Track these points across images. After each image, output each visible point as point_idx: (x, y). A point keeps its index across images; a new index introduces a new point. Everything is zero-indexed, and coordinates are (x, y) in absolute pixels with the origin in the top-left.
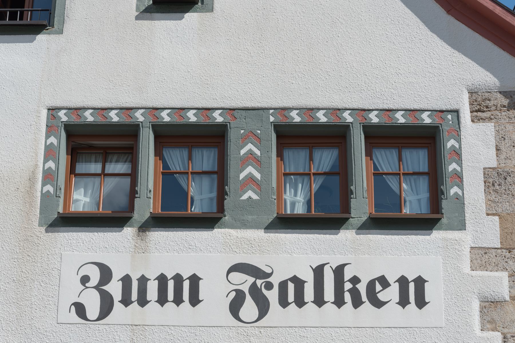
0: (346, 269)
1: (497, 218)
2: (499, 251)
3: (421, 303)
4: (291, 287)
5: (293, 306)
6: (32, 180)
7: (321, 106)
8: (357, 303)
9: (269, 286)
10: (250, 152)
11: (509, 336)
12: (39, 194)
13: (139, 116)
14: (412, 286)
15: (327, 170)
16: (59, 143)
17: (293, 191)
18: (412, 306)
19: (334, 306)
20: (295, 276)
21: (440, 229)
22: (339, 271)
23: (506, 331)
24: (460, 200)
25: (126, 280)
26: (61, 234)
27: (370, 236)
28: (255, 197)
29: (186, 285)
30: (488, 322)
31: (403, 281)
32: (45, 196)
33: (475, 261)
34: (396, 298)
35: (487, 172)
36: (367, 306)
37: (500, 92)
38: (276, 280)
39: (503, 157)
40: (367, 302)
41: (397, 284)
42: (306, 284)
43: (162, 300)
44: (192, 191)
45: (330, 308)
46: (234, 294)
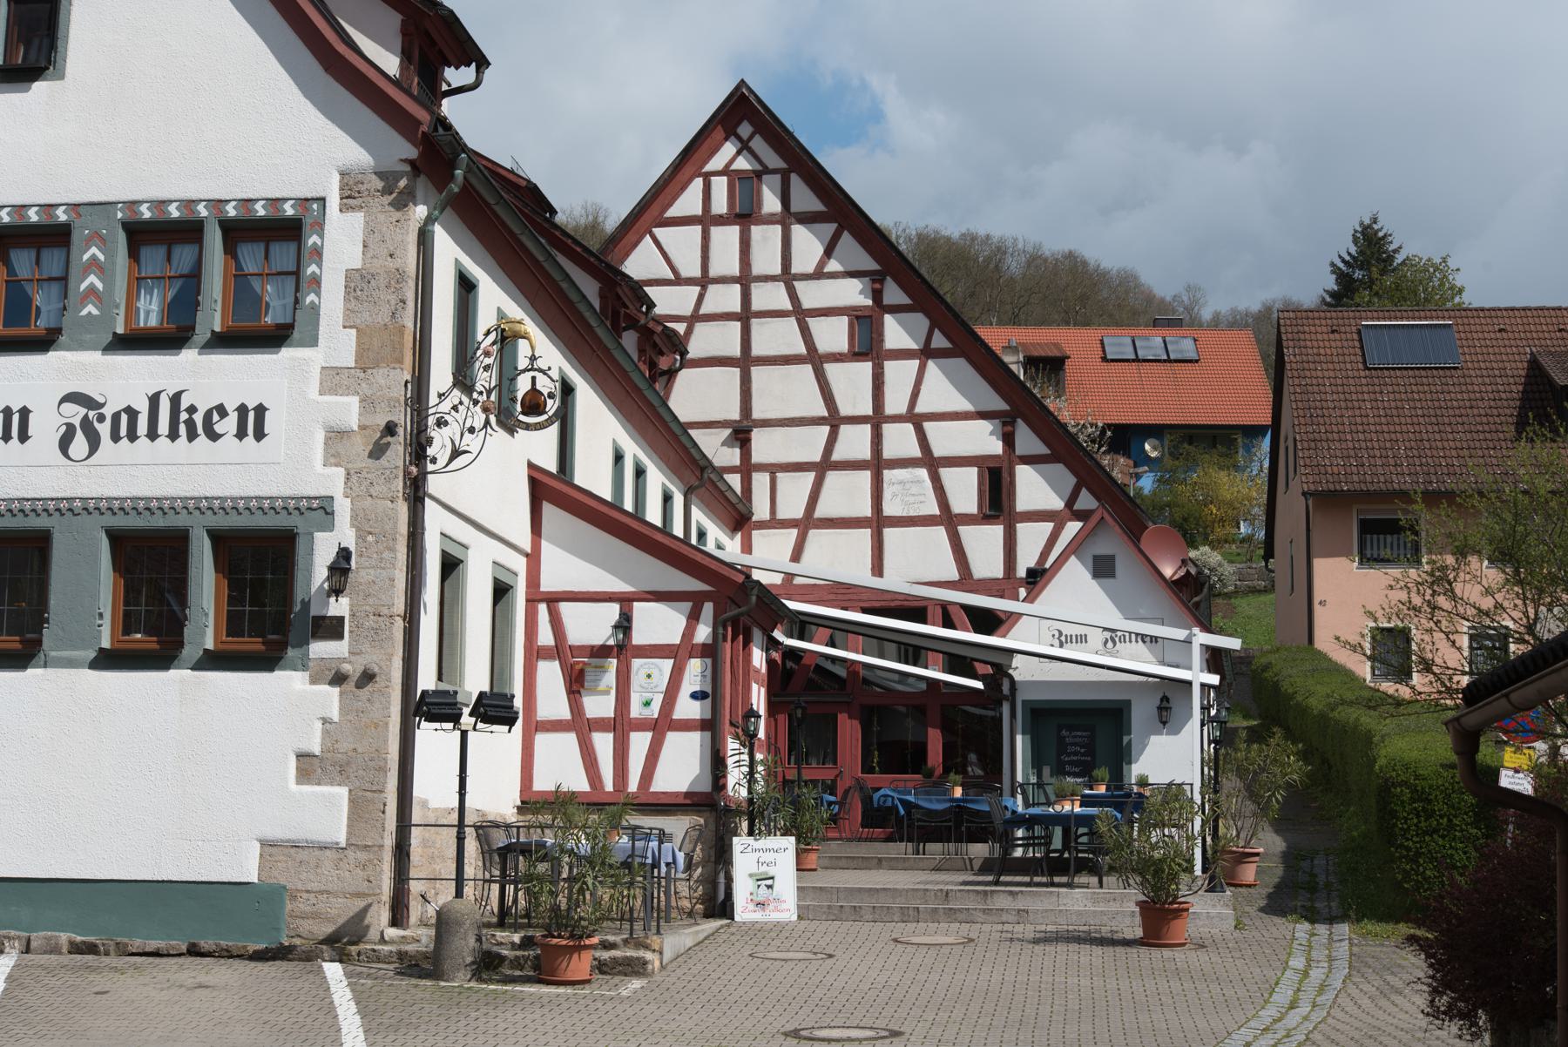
1: (354, 331)
2: (353, 371)
3: (260, 435)
4: (124, 418)
5: (125, 441)
7: (173, 198)
8: (192, 436)
9: (101, 418)
10: (94, 258)
11: (352, 472)
14: (251, 415)
15: (185, 271)
17: (148, 297)
18: (250, 439)
19: (168, 440)
20: (129, 407)
21: (290, 346)
22: (176, 399)
23: (350, 466)
24: (315, 309)
27: (213, 357)
28: (95, 312)
29: (16, 418)
30: (333, 455)
31: (242, 410)
33: (324, 384)
35: (349, 275)
36: (202, 439)
37: (375, 173)
38: (108, 411)
39: (369, 255)
40: (203, 435)
41: (236, 413)
42: (140, 415)
44: (38, 300)
45: (163, 441)
46: (64, 428)
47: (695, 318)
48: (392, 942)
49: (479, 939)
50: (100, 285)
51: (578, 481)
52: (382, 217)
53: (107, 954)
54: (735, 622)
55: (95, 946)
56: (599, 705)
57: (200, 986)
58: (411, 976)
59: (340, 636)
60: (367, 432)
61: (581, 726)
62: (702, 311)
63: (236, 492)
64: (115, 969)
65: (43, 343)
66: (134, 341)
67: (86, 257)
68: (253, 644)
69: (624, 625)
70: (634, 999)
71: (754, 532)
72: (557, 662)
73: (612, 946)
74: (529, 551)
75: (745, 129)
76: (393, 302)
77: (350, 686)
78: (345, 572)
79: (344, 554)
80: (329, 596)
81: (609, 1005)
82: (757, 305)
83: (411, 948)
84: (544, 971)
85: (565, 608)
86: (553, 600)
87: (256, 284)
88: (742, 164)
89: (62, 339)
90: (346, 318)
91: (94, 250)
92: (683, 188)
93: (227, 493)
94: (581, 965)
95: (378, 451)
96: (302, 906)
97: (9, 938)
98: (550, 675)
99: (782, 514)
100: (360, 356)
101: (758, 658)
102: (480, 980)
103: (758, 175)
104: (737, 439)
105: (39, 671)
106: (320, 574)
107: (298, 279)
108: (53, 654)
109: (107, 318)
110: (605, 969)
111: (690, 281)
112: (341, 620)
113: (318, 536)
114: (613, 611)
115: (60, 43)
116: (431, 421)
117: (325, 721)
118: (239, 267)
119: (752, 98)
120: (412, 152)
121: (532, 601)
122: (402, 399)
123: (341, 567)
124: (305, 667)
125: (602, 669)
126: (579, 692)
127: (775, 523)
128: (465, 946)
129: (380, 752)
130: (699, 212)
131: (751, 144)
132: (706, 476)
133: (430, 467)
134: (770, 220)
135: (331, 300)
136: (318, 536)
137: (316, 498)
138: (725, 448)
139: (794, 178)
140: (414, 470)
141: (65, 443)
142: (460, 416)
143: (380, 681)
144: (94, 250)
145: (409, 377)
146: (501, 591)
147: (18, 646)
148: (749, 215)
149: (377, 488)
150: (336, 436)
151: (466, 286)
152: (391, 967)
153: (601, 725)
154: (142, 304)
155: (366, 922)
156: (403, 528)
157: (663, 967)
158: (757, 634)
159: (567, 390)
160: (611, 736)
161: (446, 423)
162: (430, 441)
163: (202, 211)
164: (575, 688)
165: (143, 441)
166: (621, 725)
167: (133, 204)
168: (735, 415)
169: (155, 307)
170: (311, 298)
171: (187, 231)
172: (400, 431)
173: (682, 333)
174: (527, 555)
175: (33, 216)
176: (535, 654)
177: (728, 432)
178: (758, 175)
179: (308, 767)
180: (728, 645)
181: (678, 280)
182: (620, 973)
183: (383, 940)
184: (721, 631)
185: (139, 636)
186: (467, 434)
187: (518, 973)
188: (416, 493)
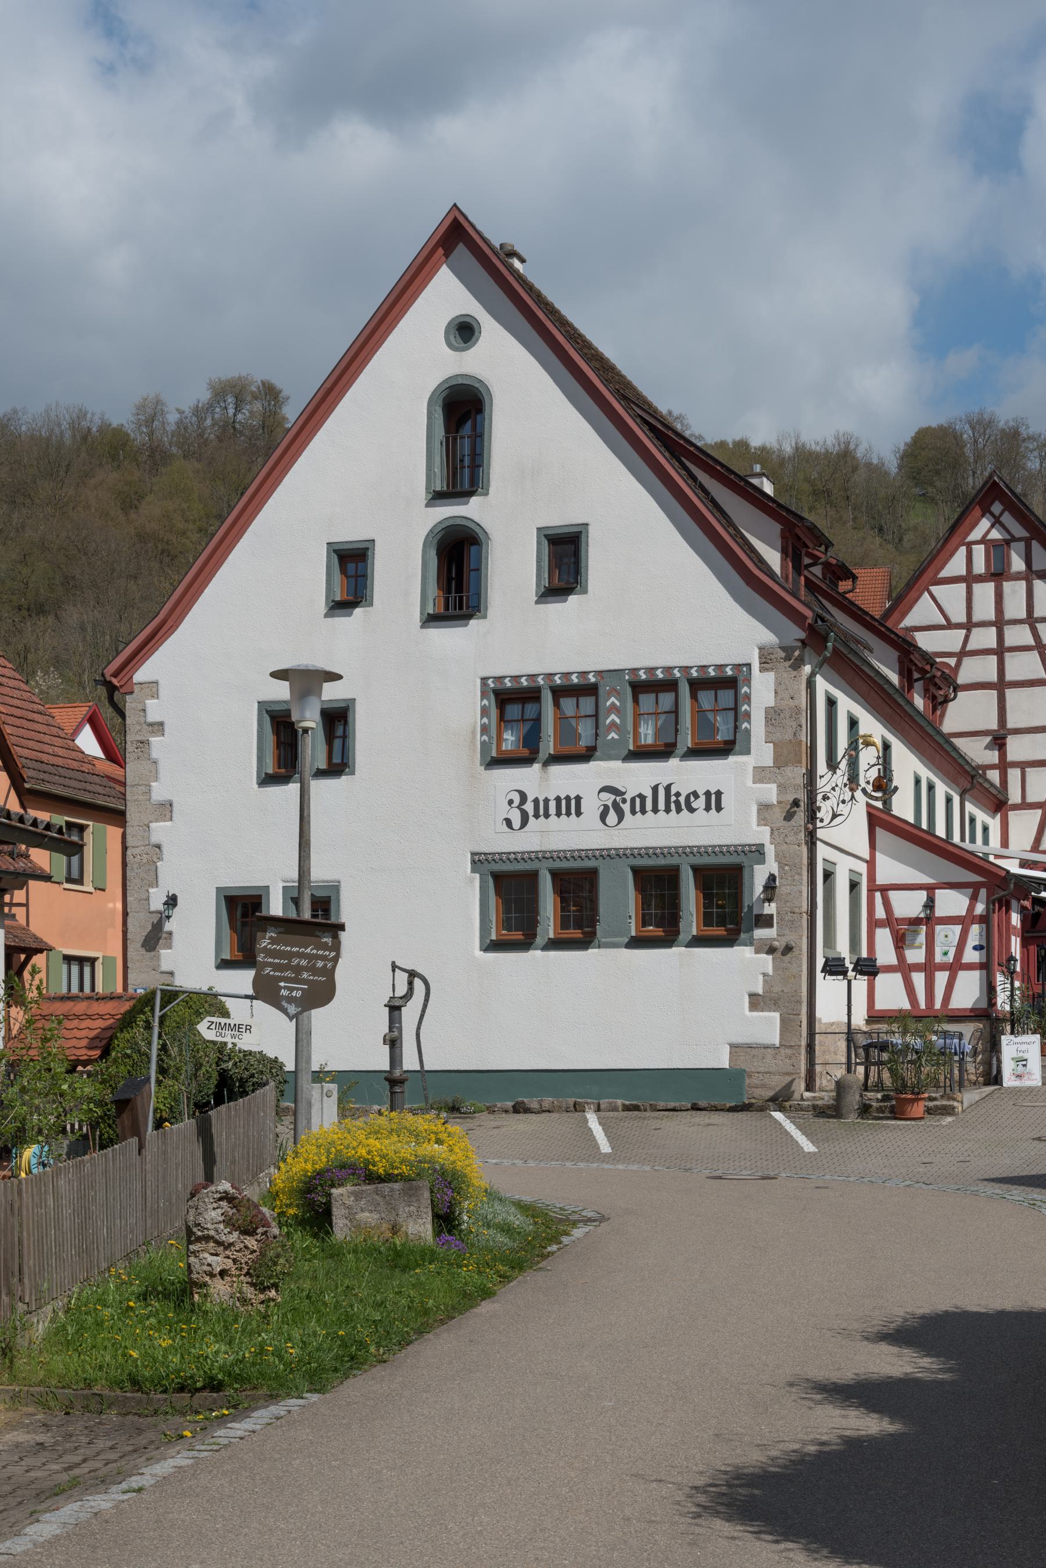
0: (673, 787)
1: (771, 745)
3: (719, 808)
4: (638, 800)
5: (639, 814)
6: (474, 733)
8: (679, 810)
9: (624, 801)
12: (479, 743)
13: (540, 681)
14: (713, 797)
16: (490, 704)
18: (713, 811)
21: (734, 755)
22: (668, 788)
24: (748, 732)
25: (536, 801)
26: (495, 771)
28: (616, 737)
29: (573, 802)
31: (708, 794)
32: (483, 743)
35: (767, 710)
36: (685, 812)
39: (778, 698)
43: (559, 814)
45: (662, 814)
46: (602, 807)
47: (963, 654)
48: (808, 1100)
49: (861, 1096)
50: (618, 721)
51: (895, 812)
52: (785, 675)
53: (645, 1110)
54: (1000, 901)
55: (639, 1106)
56: (916, 955)
57: (709, 1125)
58: (823, 1117)
59: (771, 926)
60: (783, 805)
61: (904, 969)
62: (968, 648)
64: (657, 1118)
65: (586, 756)
66: (641, 754)
67: (608, 703)
68: (720, 931)
69: (930, 905)
70: (949, 1126)
71: (1010, 813)
72: (888, 929)
73: (935, 1099)
74: (868, 859)
75: (997, 508)
76: (794, 727)
77: (778, 954)
78: (774, 888)
79: (772, 878)
80: (764, 903)
81: (937, 1129)
82: (1009, 642)
83: (819, 1103)
84: (897, 1113)
85: (893, 895)
86: (884, 889)
87: (710, 716)
88: (995, 535)
89: (597, 754)
90: (767, 736)
91: (613, 699)
92: (952, 554)
93: (701, 843)
94: (918, 1109)
95: (789, 816)
96: (755, 1081)
97: (588, 1103)
98: (884, 937)
99: (1030, 799)
101: (1015, 919)
102: (862, 1118)
103: (1008, 542)
104: (995, 744)
105: (596, 950)
106: (758, 889)
107: (737, 714)
108: (603, 940)
109: (623, 740)
110: (931, 1112)
111: (959, 626)
112: (771, 916)
113: (756, 867)
114: (923, 895)
116: (819, 797)
117: (765, 975)
118: (700, 706)
119: (1002, 484)
121: (871, 891)
122: (802, 785)
123: (770, 886)
124: (751, 944)
125: (916, 933)
126: (902, 947)
127: (1025, 805)
128: (853, 1099)
129: (797, 992)
130: (964, 572)
131: (1002, 519)
132: (975, 781)
133: (819, 824)
134: (1017, 577)
135: (757, 726)
136: (756, 867)
137: (754, 845)
138: (987, 751)
139: (1034, 543)
140: (810, 826)
142: (836, 794)
143: (796, 952)
144: (613, 699)
145: (804, 771)
146: (854, 886)
147: (581, 936)
148: (1001, 574)
149: (790, 838)
150: (764, 808)
151: (831, 703)
152: (810, 1113)
153: (917, 968)
154: (642, 730)
155: (792, 1089)
156: (805, 861)
157: (963, 1111)
158: (1014, 903)
159: (887, 747)
160: (923, 974)
161: (828, 798)
162: (819, 809)
163: (677, 673)
164: (900, 945)
165: (650, 814)
166: (929, 968)
167: (634, 671)
168: (994, 725)
169: (650, 731)
170: (745, 725)
171: (669, 685)
172: (802, 804)
173: (953, 665)
174: (867, 862)
175: (575, 679)
176: (874, 924)
177: (988, 739)
178: (1008, 542)
179: (756, 1002)
180: (996, 916)
181: (950, 625)
182: (940, 1114)
183: (802, 1099)
184: (991, 907)
185: (651, 928)
186: (841, 804)
187: (881, 1115)
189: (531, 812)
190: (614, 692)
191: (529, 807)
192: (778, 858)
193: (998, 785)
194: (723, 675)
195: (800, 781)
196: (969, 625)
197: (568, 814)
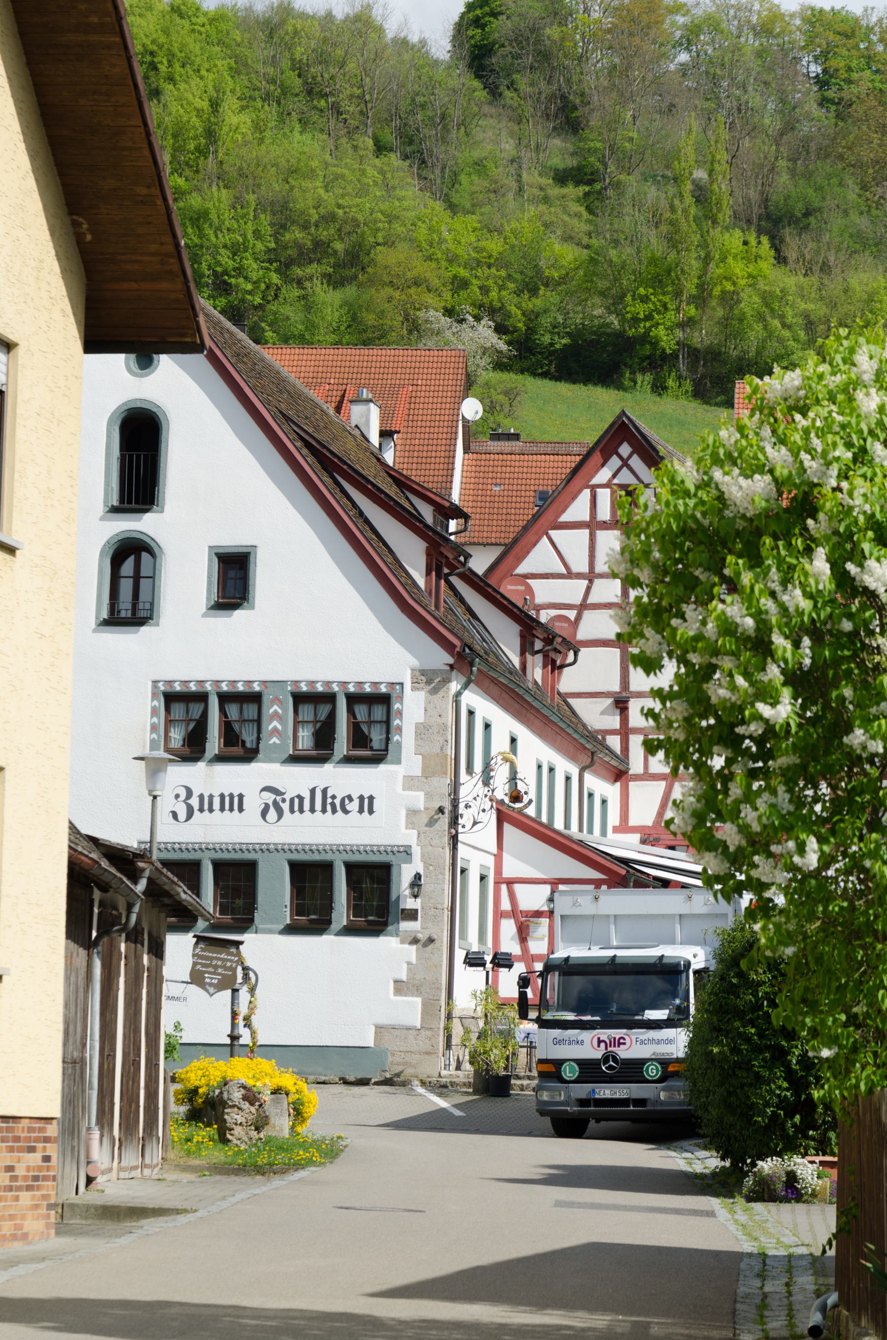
3: (371, 811)
4: (296, 801)
9: (284, 801)
10: (276, 712)
22: (325, 791)
24: (399, 744)
25: (201, 797)
28: (278, 742)
31: (361, 798)
34: (357, 809)
35: (417, 725)
36: (340, 813)
38: (287, 797)
43: (222, 809)
45: (318, 814)
47: (583, 606)
59: (416, 919)
62: (589, 602)
63: (359, 842)
77: (420, 945)
78: (420, 886)
79: (418, 876)
85: (517, 887)
86: (510, 882)
89: (260, 756)
90: (416, 749)
92: (574, 498)
100: (424, 769)
105: (254, 935)
111: (579, 576)
112: (416, 911)
113: (403, 866)
115: (251, 588)
116: (462, 806)
117: (409, 963)
120: (451, 661)
121: (497, 883)
123: (416, 882)
124: (397, 935)
129: (438, 980)
130: (587, 518)
131: (630, 462)
133: (460, 829)
140: (453, 831)
141: (264, 813)
142: (478, 803)
143: (437, 944)
150: (412, 813)
154: (301, 733)
162: (462, 816)
165: (307, 813)
167: (296, 683)
168: (616, 687)
172: (446, 811)
176: (499, 915)
179: (400, 987)
181: (570, 575)
188: (454, 840)
189: (196, 806)
190: (277, 700)
191: (194, 802)
192: (424, 859)
193: (618, 752)
194: (378, 691)
195: (446, 790)
196: (591, 576)
197: (231, 809)
